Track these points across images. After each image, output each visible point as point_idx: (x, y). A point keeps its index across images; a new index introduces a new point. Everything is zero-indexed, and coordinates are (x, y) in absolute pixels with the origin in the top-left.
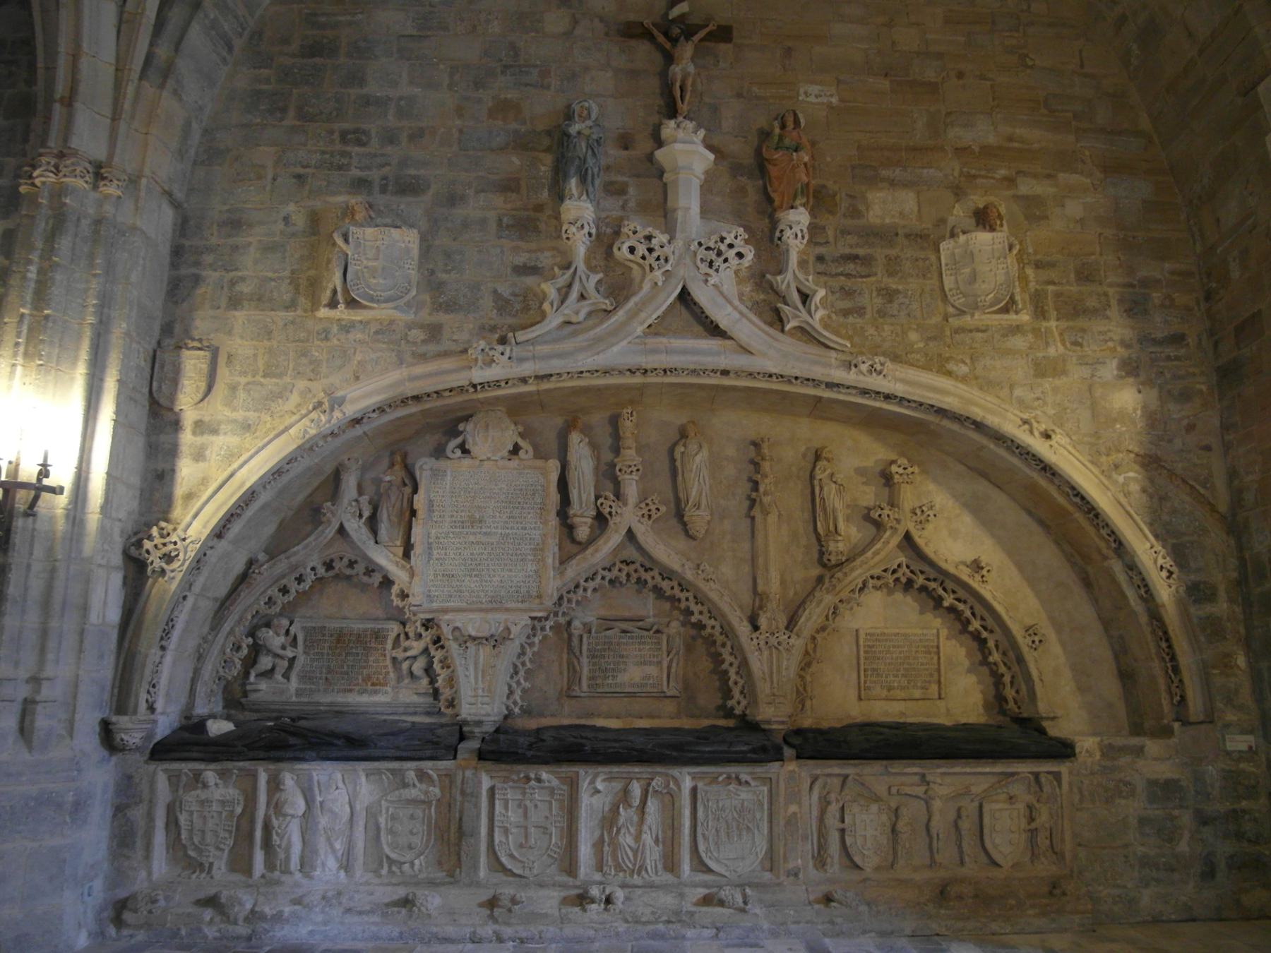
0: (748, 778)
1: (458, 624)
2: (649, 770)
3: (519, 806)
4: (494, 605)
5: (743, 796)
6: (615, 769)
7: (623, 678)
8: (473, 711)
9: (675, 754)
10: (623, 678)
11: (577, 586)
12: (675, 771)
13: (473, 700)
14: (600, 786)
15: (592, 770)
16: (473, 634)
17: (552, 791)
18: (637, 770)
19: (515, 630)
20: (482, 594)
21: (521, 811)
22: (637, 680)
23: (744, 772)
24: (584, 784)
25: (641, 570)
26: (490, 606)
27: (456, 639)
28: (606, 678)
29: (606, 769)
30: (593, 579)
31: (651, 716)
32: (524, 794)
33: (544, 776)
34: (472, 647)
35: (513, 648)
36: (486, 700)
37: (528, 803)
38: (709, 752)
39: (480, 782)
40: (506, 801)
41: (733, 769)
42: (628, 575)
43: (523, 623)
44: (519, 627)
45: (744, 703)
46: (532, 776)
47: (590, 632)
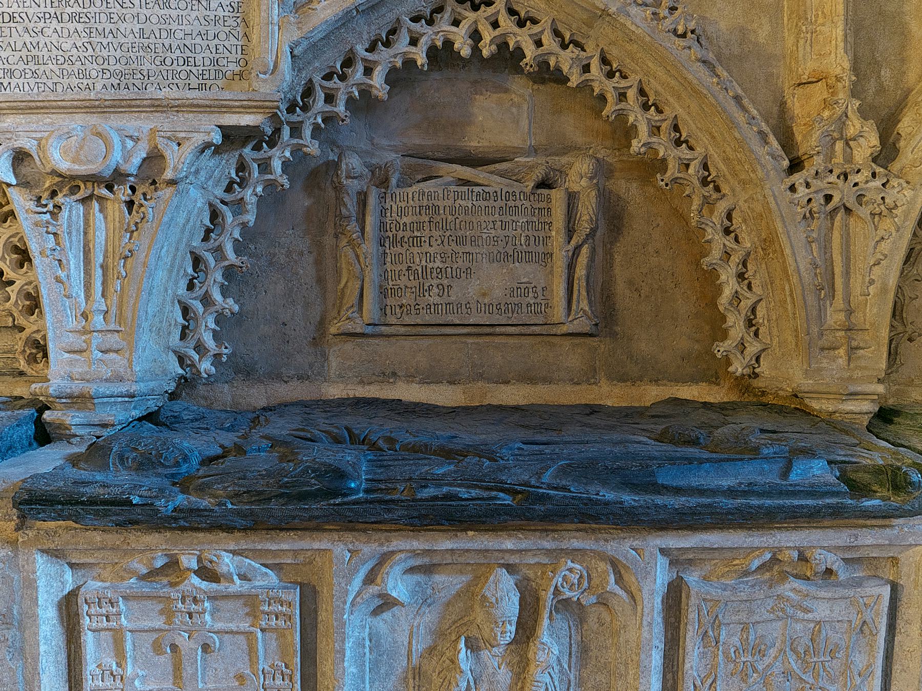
0: (832, 560)
1: (28, 144)
2: (547, 544)
3: (157, 648)
4: (124, 94)
5: (822, 611)
6: (445, 543)
7: (469, 290)
8: (78, 370)
9: (628, 498)
10: (469, 290)
11: (348, 62)
12: (623, 546)
13: (78, 341)
14: (398, 585)
15: (370, 548)
16: (64, 166)
17: (251, 602)
18: (509, 544)
19: (177, 160)
20: (93, 69)
21: (165, 660)
22: (498, 293)
23: (823, 543)
24: (346, 591)
25: (507, 23)
26: (111, 94)
27: (24, 184)
28: (423, 290)
29: (417, 543)
30: (387, 44)
31: (528, 378)
32: (168, 614)
33: (227, 563)
34: (72, 210)
35: (178, 214)
36: (114, 340)
37: (182, 640)
38: (731, 492)
39: (30, 584)
40: (118, 636)
41: (788, 540)
42: (476, 36)
43: (199, 139)
44: (188, 150)
45: (753, 348)
46: (189, 561)
47: (383, 183)
